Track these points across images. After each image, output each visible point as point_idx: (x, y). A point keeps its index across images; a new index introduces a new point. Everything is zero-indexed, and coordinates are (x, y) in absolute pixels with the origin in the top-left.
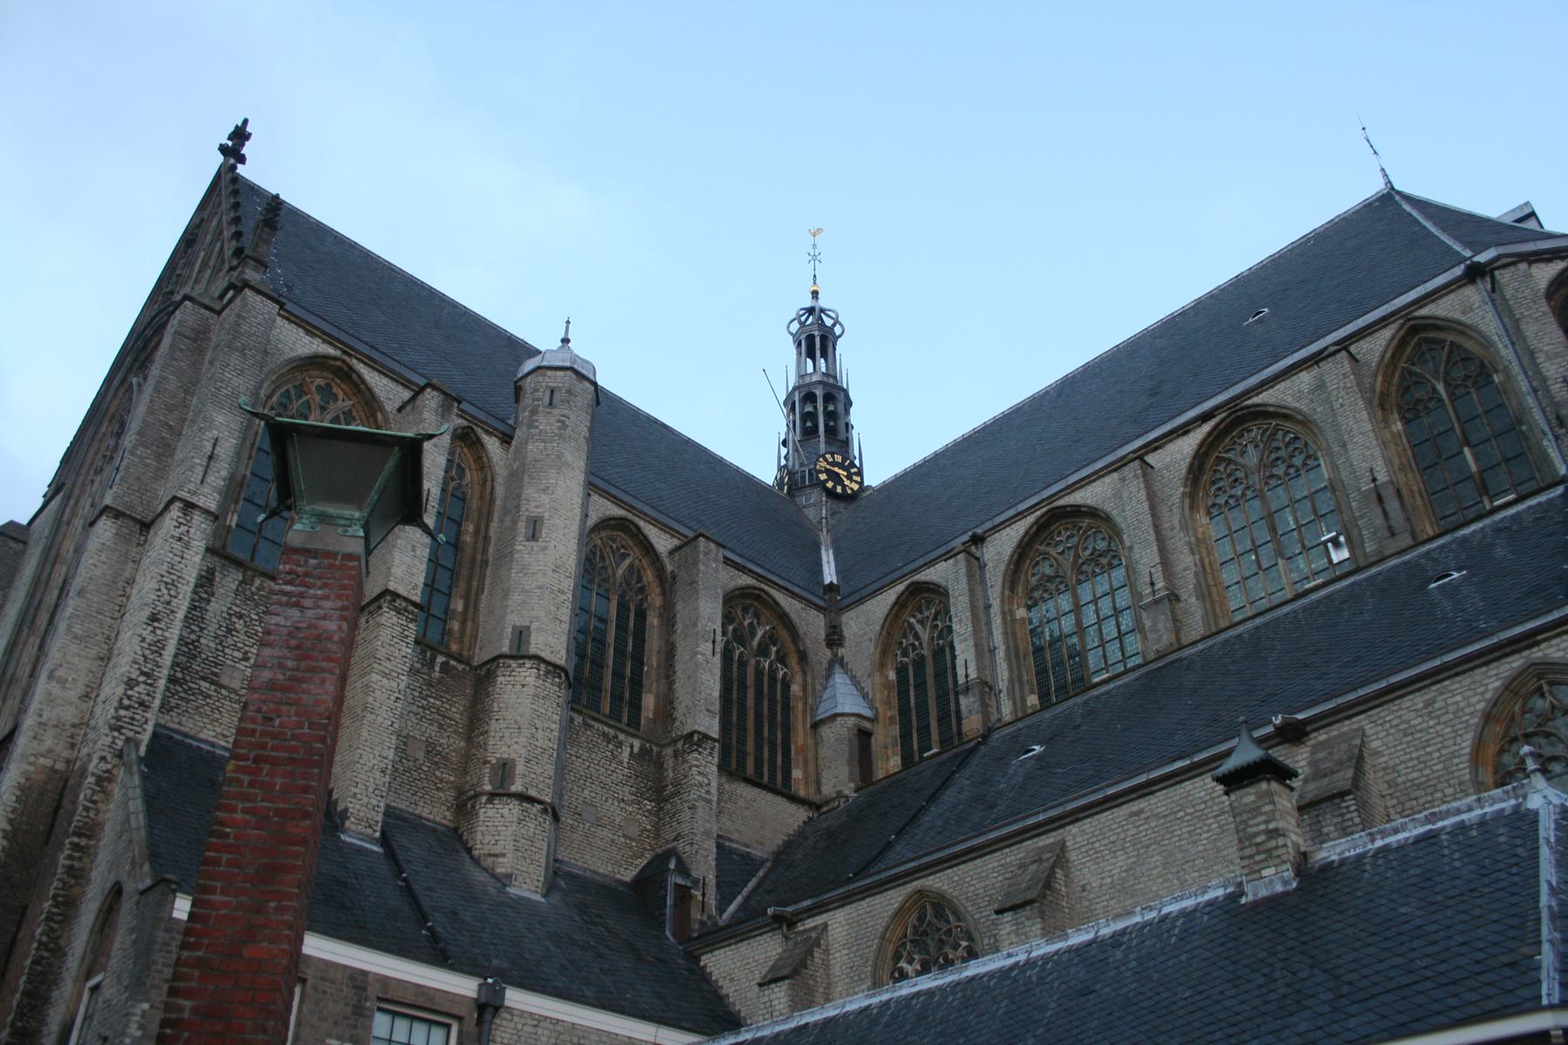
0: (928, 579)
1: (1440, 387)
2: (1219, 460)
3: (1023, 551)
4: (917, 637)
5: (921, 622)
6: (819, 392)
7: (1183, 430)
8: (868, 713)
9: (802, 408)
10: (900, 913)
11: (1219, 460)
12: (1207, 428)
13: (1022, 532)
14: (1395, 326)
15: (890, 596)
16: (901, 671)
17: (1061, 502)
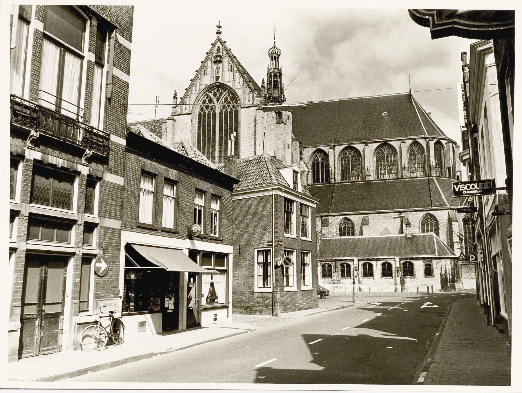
0: (323, 149)
1: (416, 152)
2: (380, 149)
3: (343, 150)
4: (318, 158)
5: (319, 155)
6: (278, 74)
7: (376, 142)
8: (308, 171)
9: (274, 79)
10: (343, 219)
11: (380, 149)
12: (379, 143)
13: (343, 148)
14: (413, 140)
15: (314, 149)
16: (314, 163)
17: (352, 145)
